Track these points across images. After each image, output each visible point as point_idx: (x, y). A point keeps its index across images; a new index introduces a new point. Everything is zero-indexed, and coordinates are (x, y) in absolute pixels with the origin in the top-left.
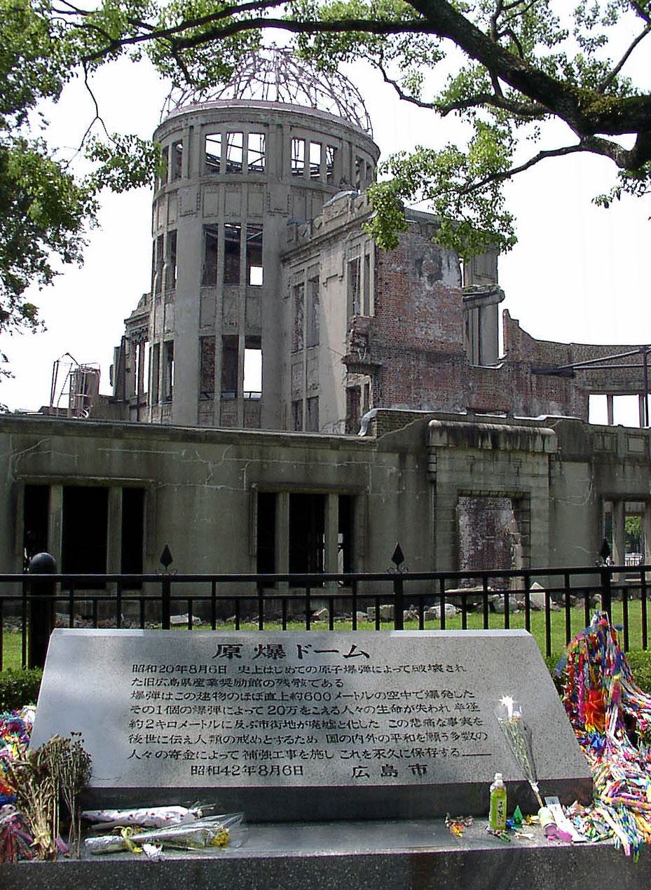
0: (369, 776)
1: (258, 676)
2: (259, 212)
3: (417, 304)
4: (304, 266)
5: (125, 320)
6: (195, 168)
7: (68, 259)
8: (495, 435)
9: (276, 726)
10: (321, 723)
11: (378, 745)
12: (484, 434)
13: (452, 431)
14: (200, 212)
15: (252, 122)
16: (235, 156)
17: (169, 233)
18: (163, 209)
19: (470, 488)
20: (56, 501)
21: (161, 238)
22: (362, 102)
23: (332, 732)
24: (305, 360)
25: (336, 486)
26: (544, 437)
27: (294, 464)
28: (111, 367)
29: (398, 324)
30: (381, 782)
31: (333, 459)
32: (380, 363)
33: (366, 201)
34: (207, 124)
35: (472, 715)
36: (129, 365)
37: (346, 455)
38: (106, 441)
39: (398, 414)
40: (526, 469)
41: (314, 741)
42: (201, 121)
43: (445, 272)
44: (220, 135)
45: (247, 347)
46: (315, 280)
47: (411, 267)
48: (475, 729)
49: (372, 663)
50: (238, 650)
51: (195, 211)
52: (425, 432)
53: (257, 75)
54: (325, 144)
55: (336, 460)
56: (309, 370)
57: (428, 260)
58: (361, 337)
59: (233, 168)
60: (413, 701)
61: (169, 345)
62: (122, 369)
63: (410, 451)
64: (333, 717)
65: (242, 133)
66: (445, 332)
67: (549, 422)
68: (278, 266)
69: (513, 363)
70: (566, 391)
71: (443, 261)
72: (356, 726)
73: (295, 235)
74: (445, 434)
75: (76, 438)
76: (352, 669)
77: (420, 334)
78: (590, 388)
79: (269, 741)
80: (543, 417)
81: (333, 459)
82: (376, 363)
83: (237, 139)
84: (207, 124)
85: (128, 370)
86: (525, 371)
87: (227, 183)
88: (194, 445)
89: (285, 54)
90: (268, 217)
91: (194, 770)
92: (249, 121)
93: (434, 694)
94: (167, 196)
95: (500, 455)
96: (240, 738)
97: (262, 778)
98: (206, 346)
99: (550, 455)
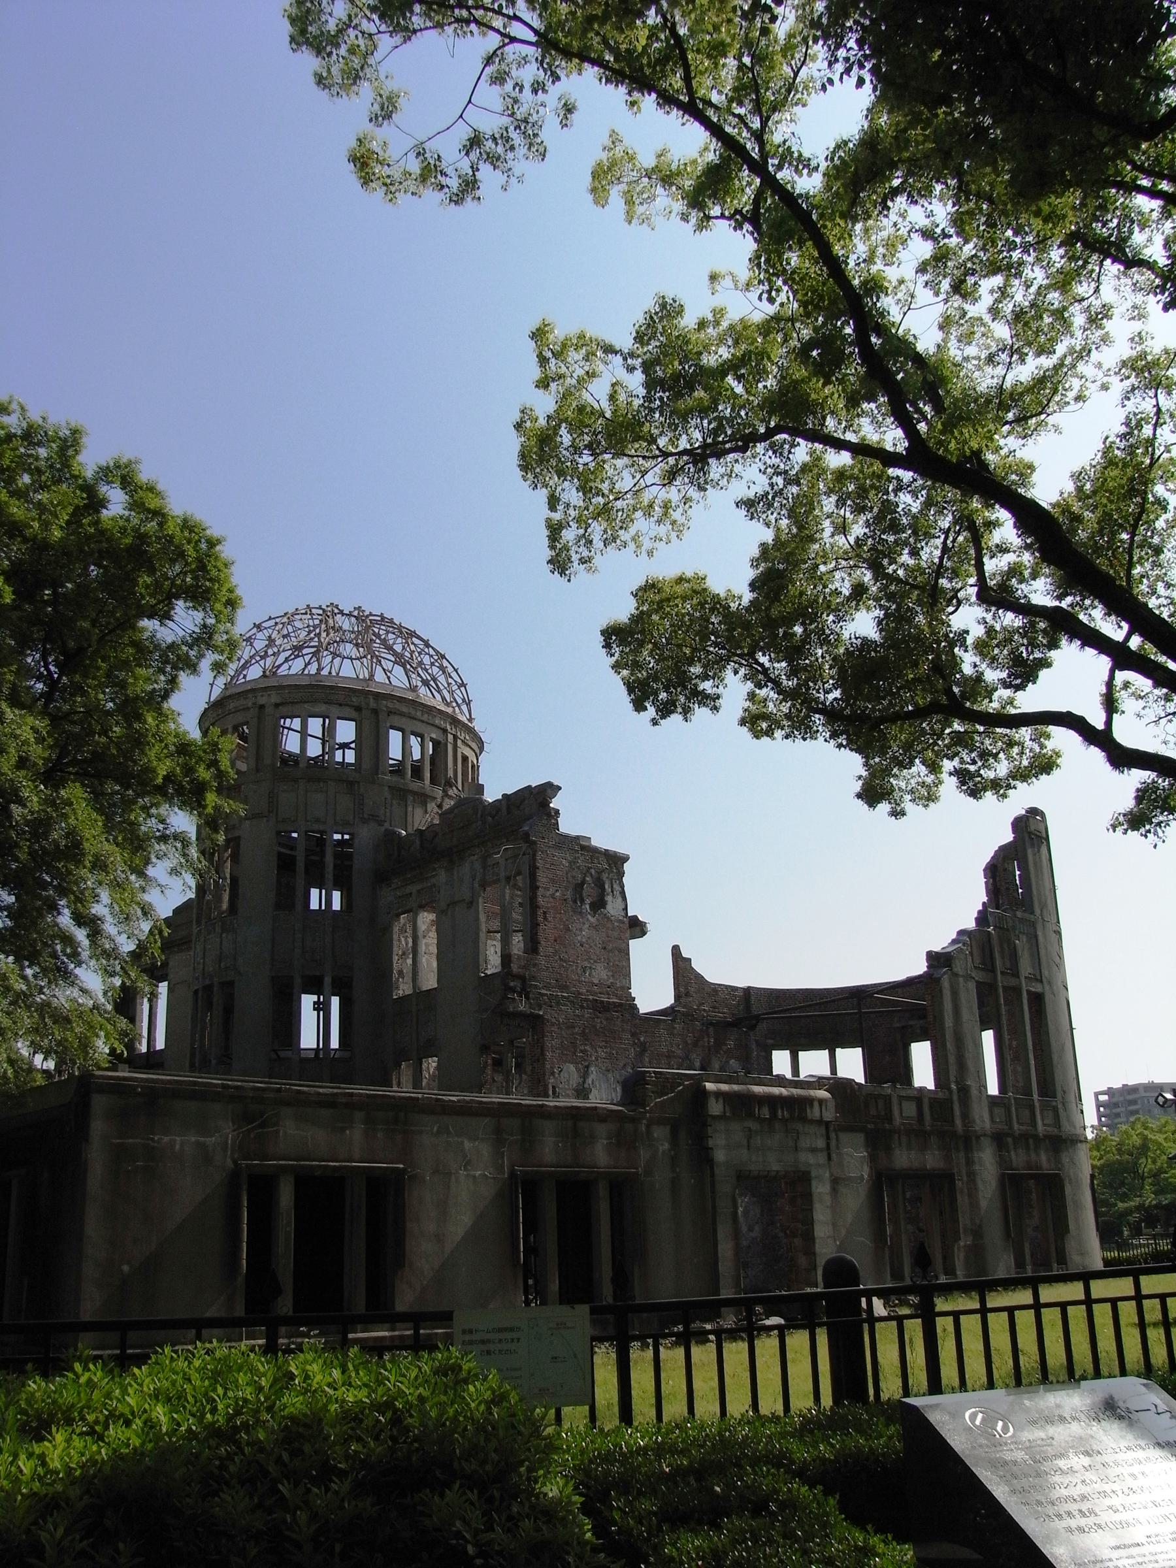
4: (413, 888)
15: (340, 705)
20: (286, 1196)
26: (821, 1102)
33: (504, 809)
34: (282, 704)
40: (805, 1142)
42: (274, 698)
43: (609, 898)
54: (427, 739)
74: (721, 1100)
84: (282, 704)
95: (777, 1126)
99: (827, 1124)
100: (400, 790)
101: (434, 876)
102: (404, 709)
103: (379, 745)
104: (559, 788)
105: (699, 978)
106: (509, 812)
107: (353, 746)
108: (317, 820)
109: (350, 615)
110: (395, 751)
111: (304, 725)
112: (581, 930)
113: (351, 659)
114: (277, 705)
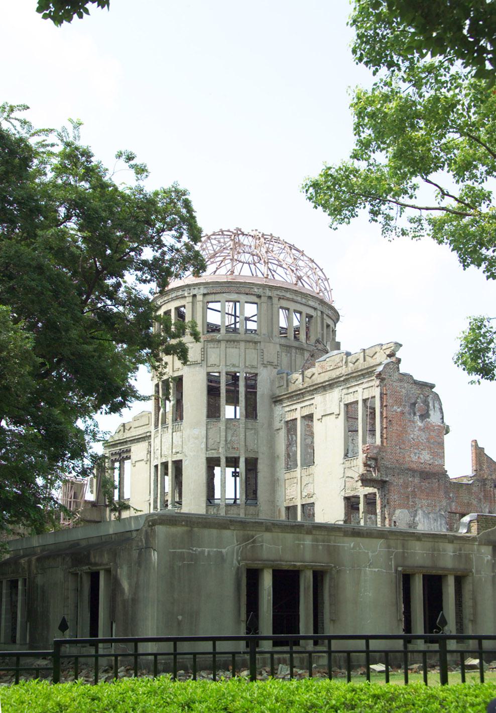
2: (255, 363)
4: (298, 406)
15: (247, 294)
25: (453, 569)
27: (424, 553)
31: (449, 549)
37: (458, 546)
46: (310, 417)
55: (452, 551)
66: (431, 457)
73: (285, 382)
75: (280, 534)
77: (415, 458)
81: (449, 549)
88: (358, 539)
90: (262, 368)
92: (245, 293)
100: (287, 346)
101: (312, 399)
103: (273, 319)
107: (255, 318)
110: (283, 323)
111: (223, 307)
113: (249, 264)
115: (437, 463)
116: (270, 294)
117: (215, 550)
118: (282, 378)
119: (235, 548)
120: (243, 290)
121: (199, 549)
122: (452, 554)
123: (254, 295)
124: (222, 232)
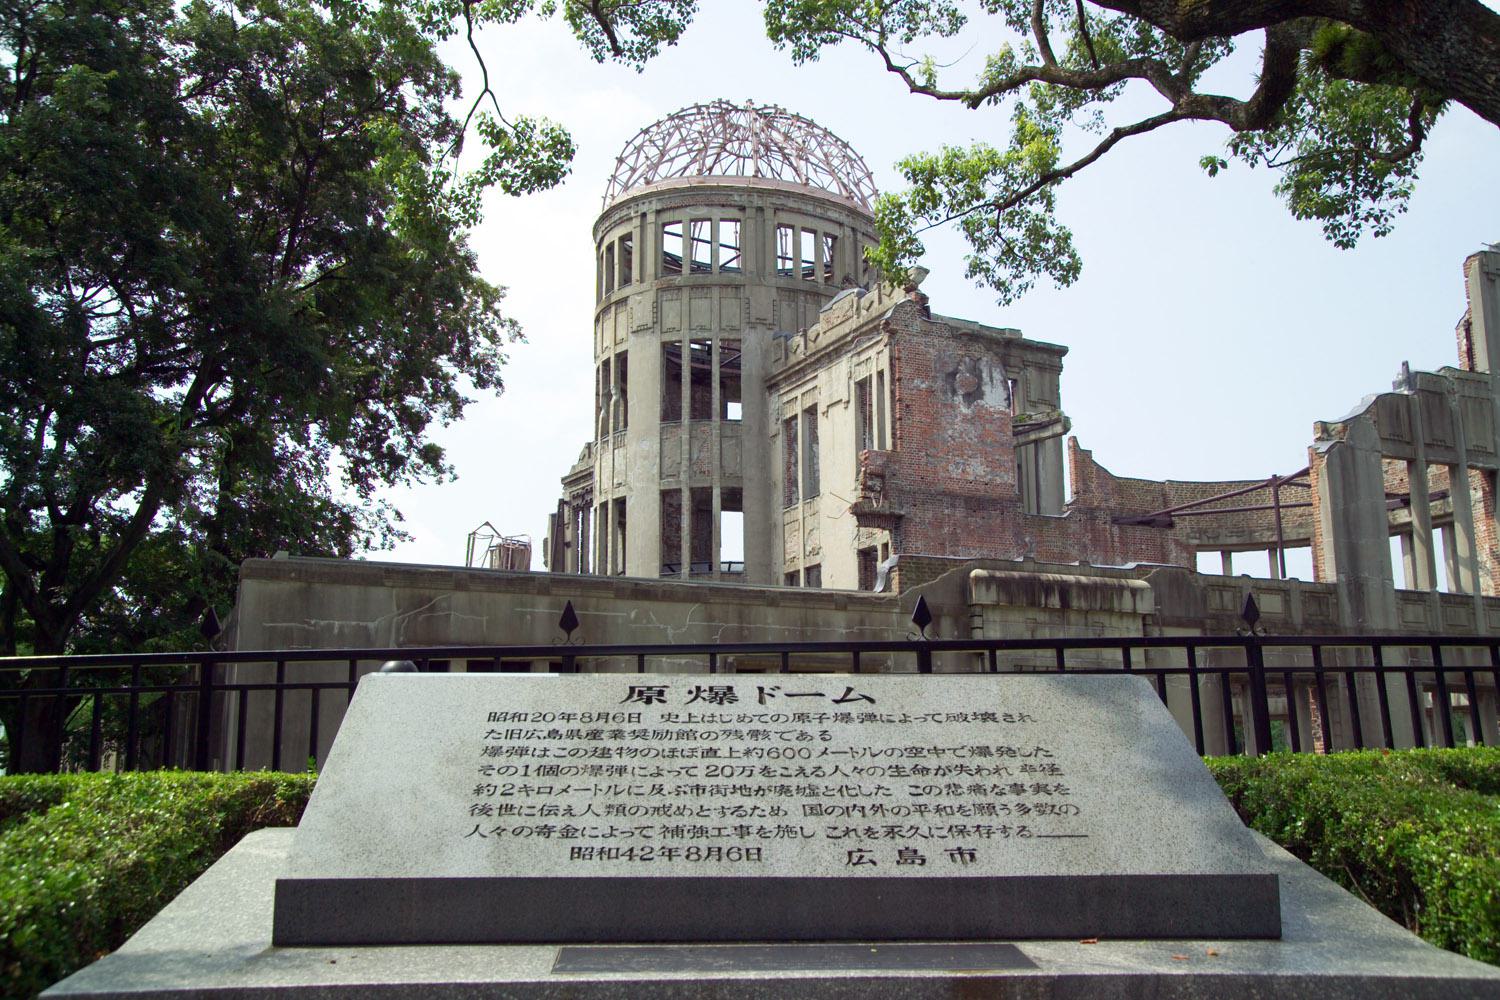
0: (874, 863)
1: (691, 726)
2: (736, 323)
3: (950, 432)
4: (798, 393)
5: (563, 480)
6: (650, 268)
7: (481, 383)
8: (1064, 589)
9: (718, 792)
10: (793, 789)
11: (891, 820)
12: (1048, 588)
13: (1004, 585)
14: (658, 327)
15: (723, 206)
16: (703, 254)
17: (618, 356)
18: (609, 323)
19: (1032, 663)
21: (606, 363)
22: (869, 175)
23: (812, 801)
24: (801, 518)
26: (1134, 591)
28: (546, 541)
29: (924, 460)
30: (897, 872)
32: (902, 513)
35: (1052, 781)
36: (569, 535)
37: (856, 617)
38: (527, 598)
39: (926, 561)
41: (781, 813)
42: (656, 205)
43: (986, 389)
44: (680, 225)
45: (724, 508)
46: (811, 411)
47: (940, 383)
48: (1056, 799)
49: (877, 709)
50: (661, 693)
51: (650, 325)
52: (964, 587)
53: (728, 147)
54: (820, 233)
55: (843, 624)
56: (807, 531)
57: (964, 375)
58: (876, 477)
59: (698, 268)
60: (948, 759)
61: (621, 503)
62: (558, 544)
63: (945, 610)
64: (813, 780)
65: (710, 220)
66: (989, 469)
67: (1139, 572)
68: (763, 394)
69: (1085, 510)
70: (1162, 546)
71: (984, 375)
72: (853, 792)
74: (994, 588)
75: (485, 595)
76: (846, 718)
77: (956, 473)
78: (1196, 542)
79: (706, 813)
80: (1131, 565)
82: (897, 512)
83: (704, 230)
85: (568, 545)
86: (1102, 522)
87: (693, 287)
88: (646, 604)
89: (765, 116)
91: (577, 853)
93: (984, 751)
94: (613, 308)
95: (1073, 617)
96: (657, 809)
97: (690, 865)
98: (669, 498)
99: (1144, 617)
102: (791, 204)
104: (927, 272)
105: (1103, 472)
106: (880, 302)
108: (702, 328)
109: (744, 111)
112: (953, 424)
114: (658, 212)
115: (999, 481)
116: (760, 204)
117: (354, 623)
118: (779, 345)
119: (395, 620)
120: (716, 199)
121: (322, 623)
122: (844, 631)
123: (735, 206)
124: (698, 107)
